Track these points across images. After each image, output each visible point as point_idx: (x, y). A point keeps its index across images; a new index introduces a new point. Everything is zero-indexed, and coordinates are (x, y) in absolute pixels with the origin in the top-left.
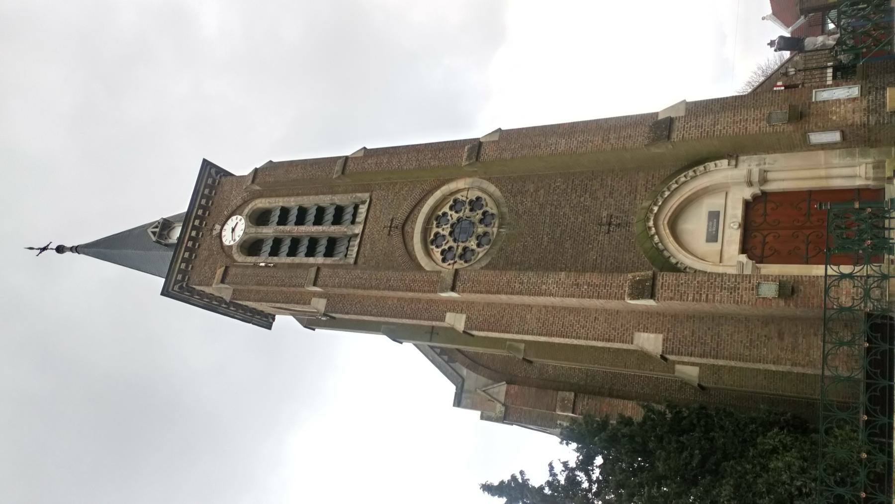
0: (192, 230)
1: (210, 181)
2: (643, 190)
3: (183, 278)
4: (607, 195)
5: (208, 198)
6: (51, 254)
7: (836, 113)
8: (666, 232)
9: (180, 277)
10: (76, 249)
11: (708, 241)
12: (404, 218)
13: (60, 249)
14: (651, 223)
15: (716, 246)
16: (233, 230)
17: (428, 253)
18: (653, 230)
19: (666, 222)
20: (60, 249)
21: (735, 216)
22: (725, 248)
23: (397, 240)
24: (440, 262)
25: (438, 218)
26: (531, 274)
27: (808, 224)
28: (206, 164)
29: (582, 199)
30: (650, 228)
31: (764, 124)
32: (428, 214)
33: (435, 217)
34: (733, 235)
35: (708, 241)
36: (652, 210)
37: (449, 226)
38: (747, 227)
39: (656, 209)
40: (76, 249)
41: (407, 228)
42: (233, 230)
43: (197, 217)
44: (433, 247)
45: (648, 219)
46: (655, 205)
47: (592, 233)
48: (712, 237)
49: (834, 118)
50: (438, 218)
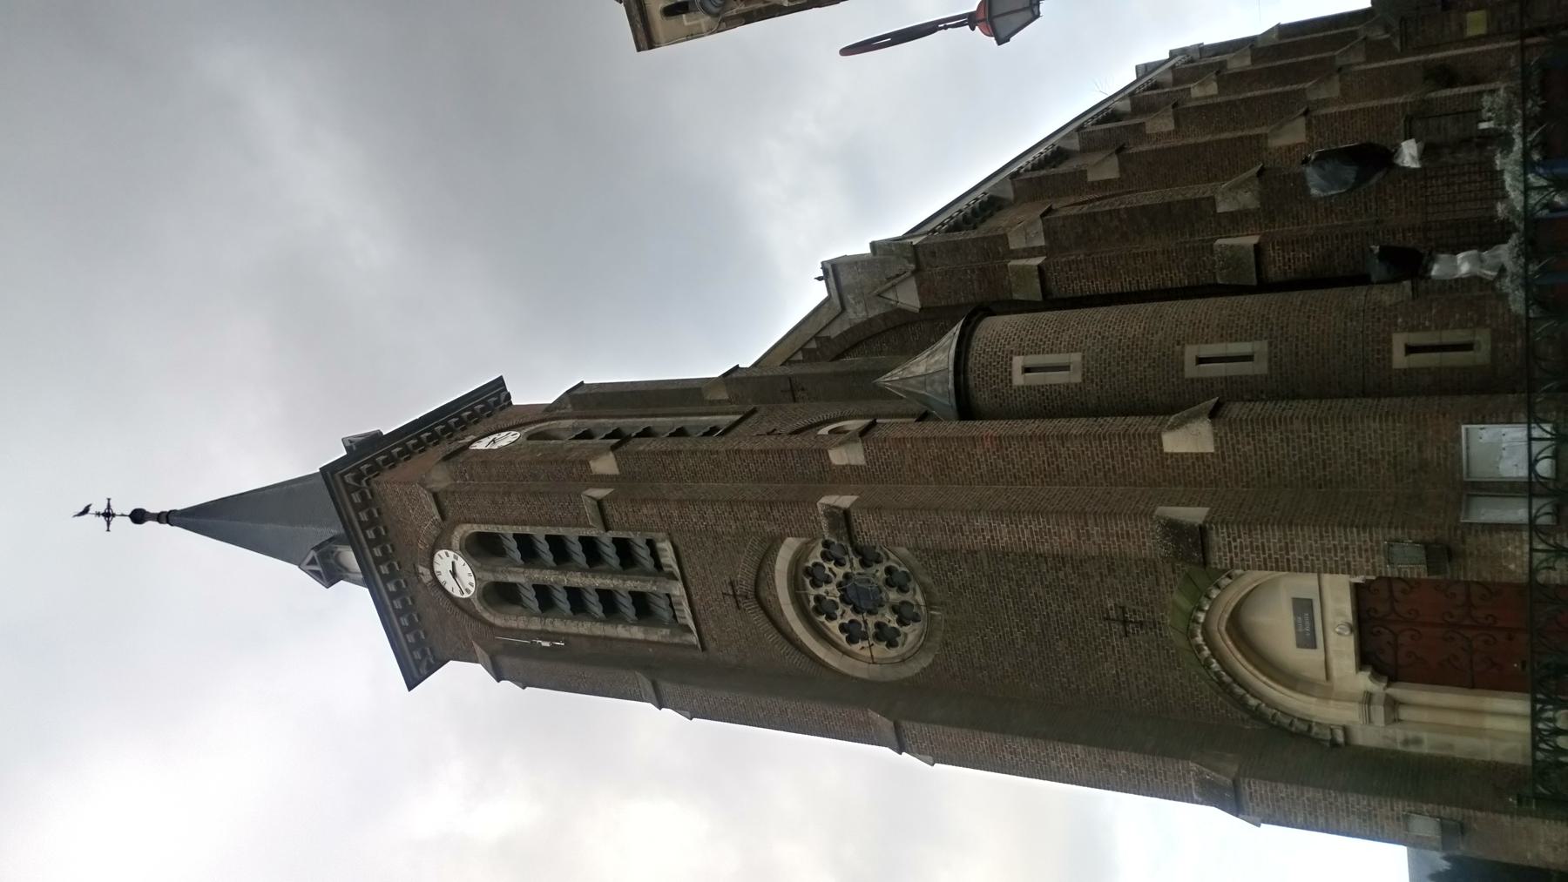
0: (349, 494)
1: (356, 498)
2: (1169, 570)
3: (424, 654)
4: (1105, 572)
5: (373, 522)
6: (122, 524)
7: (1514, 557)
8: (1226, 645)
9: (417, 655)
10: (166, 518)
11: (1299, 646)
12: (752, 576)
13: (138, 516)
14: (1200, 639)
15: (1316, 655)
16: (454, 574)
17: (821, 635)
18: (1206, 652)
19: (1223, 629)
20: (138, 516)
21: (1340, 613)
22: (1331, 654)
23: (757, 618)
24: (844, 643)
25: (818, 611)
26: (1025, 742)
27: (1467, 622)
28: (412, 683)
29: (1061, 575)
30: (1199, 649)
31: (1380, 559)
32: (790, 571)
33: (804, 574)
34: (1342, 647)
35: (1299, 646)
36: (1196, 621)
37: (841, 606)
38: (1364, 624)
39: (1202, 617)
40: (166, 518)
41: (763, 594)
42: (454, 574)
43: (378, 562)
44: (823, 618)
45: (1194, 636)
46: (1200, 609)
47: (1097, 633)
48: (1307, 640)
49: (1512, 567)
50: (808, 572)
